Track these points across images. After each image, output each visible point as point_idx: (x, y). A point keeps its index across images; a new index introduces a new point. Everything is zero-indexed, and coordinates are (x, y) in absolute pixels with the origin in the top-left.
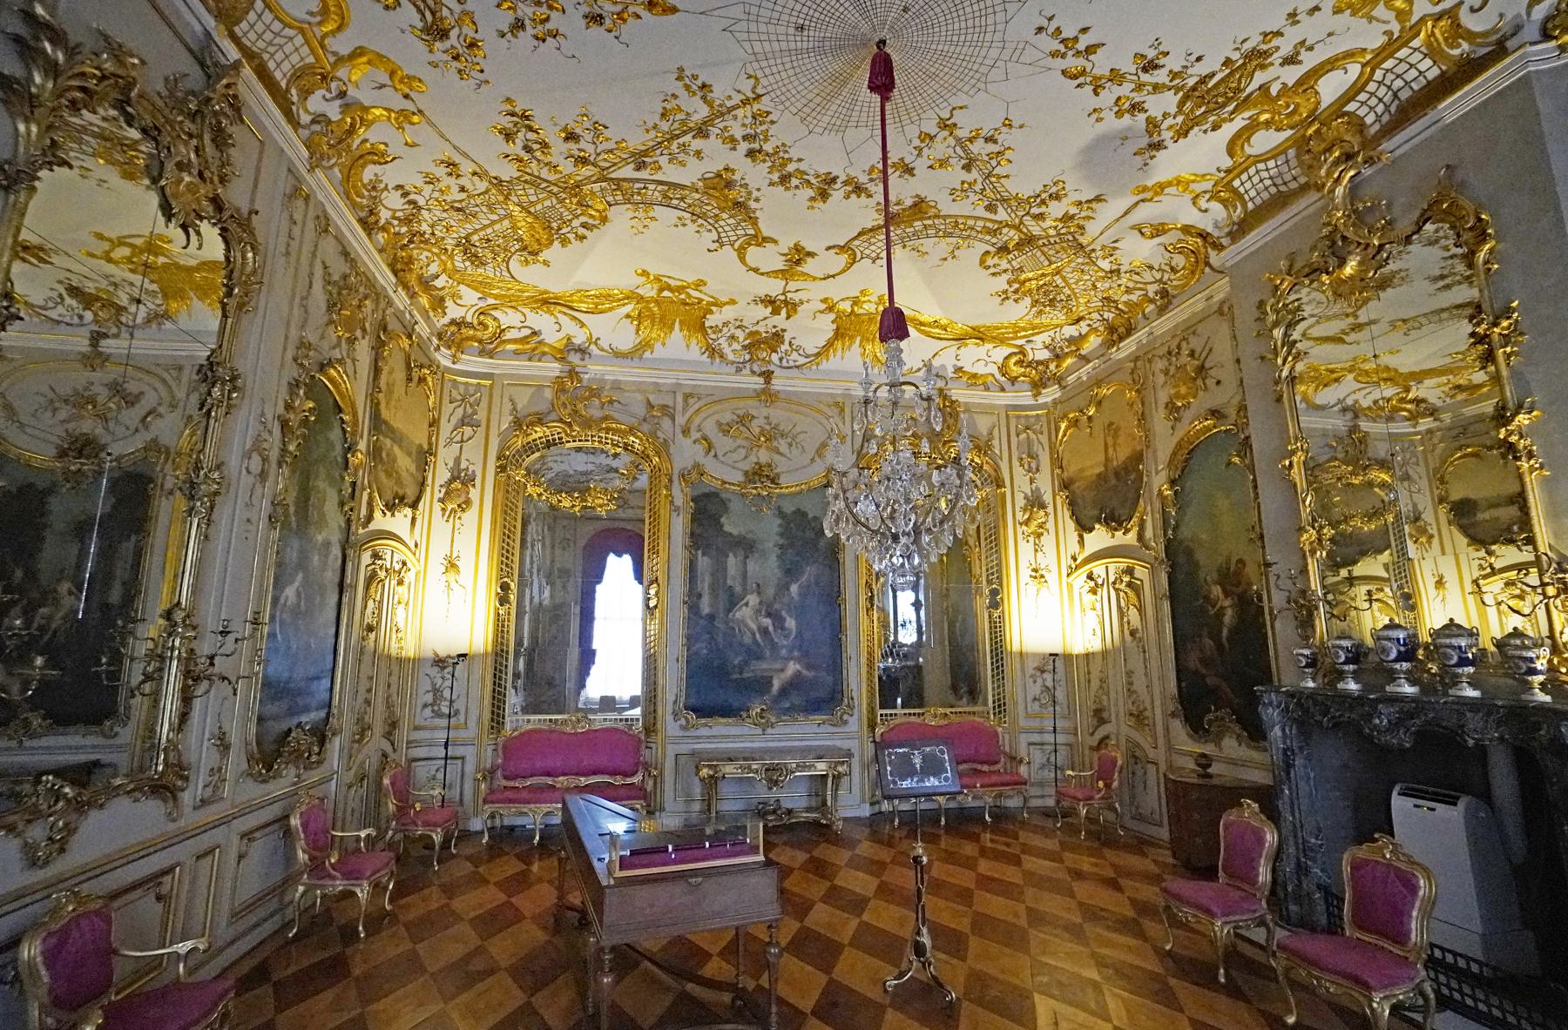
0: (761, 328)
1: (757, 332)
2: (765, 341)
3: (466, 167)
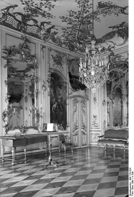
3: (66, 28)
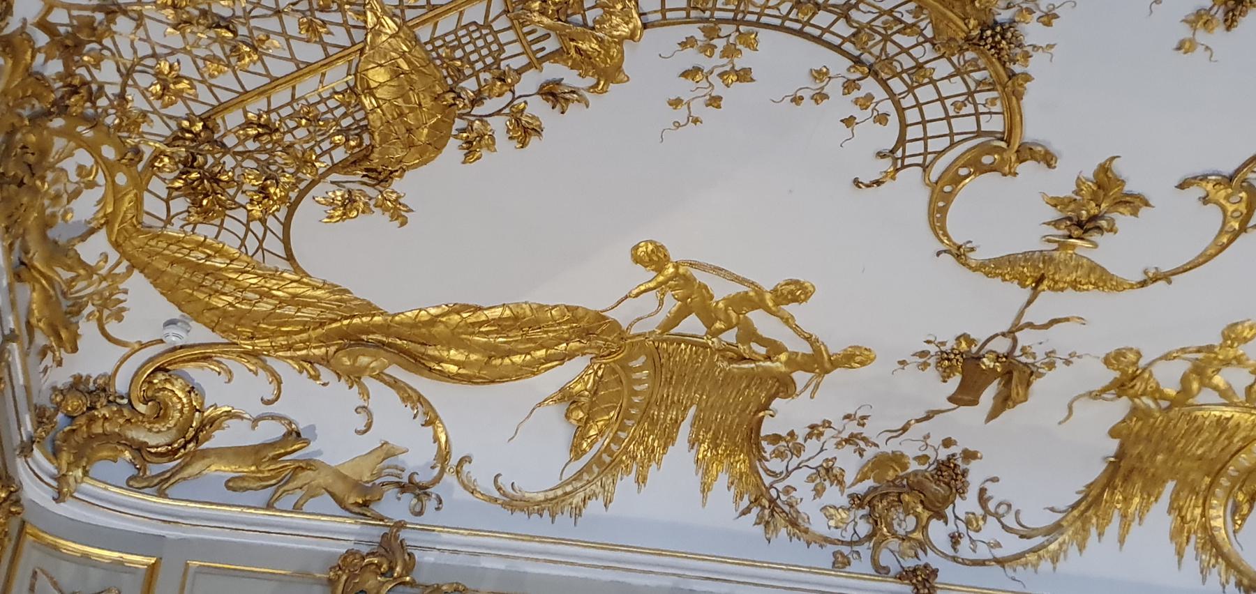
0: (909, 448)
1: (898, 459)
2: (915, 486)
